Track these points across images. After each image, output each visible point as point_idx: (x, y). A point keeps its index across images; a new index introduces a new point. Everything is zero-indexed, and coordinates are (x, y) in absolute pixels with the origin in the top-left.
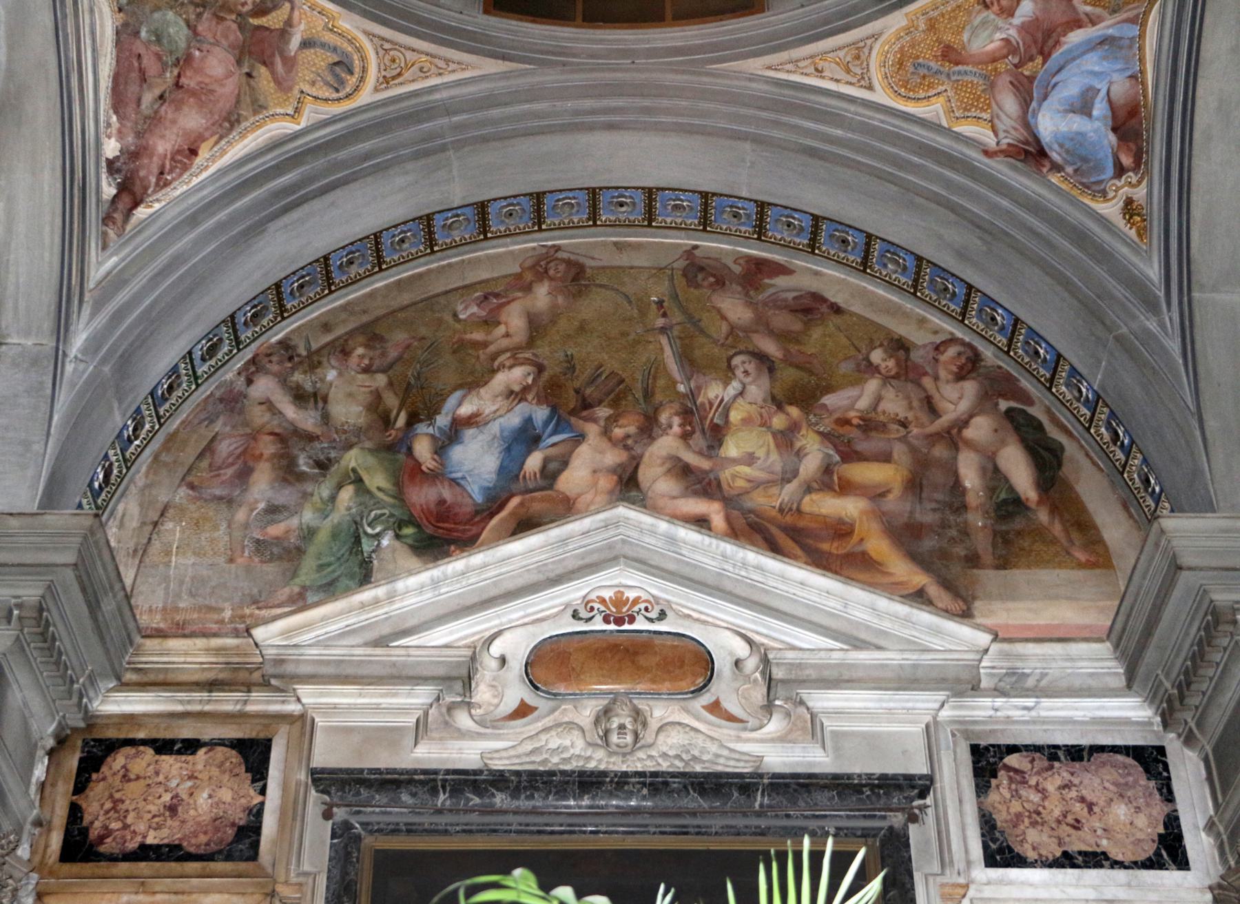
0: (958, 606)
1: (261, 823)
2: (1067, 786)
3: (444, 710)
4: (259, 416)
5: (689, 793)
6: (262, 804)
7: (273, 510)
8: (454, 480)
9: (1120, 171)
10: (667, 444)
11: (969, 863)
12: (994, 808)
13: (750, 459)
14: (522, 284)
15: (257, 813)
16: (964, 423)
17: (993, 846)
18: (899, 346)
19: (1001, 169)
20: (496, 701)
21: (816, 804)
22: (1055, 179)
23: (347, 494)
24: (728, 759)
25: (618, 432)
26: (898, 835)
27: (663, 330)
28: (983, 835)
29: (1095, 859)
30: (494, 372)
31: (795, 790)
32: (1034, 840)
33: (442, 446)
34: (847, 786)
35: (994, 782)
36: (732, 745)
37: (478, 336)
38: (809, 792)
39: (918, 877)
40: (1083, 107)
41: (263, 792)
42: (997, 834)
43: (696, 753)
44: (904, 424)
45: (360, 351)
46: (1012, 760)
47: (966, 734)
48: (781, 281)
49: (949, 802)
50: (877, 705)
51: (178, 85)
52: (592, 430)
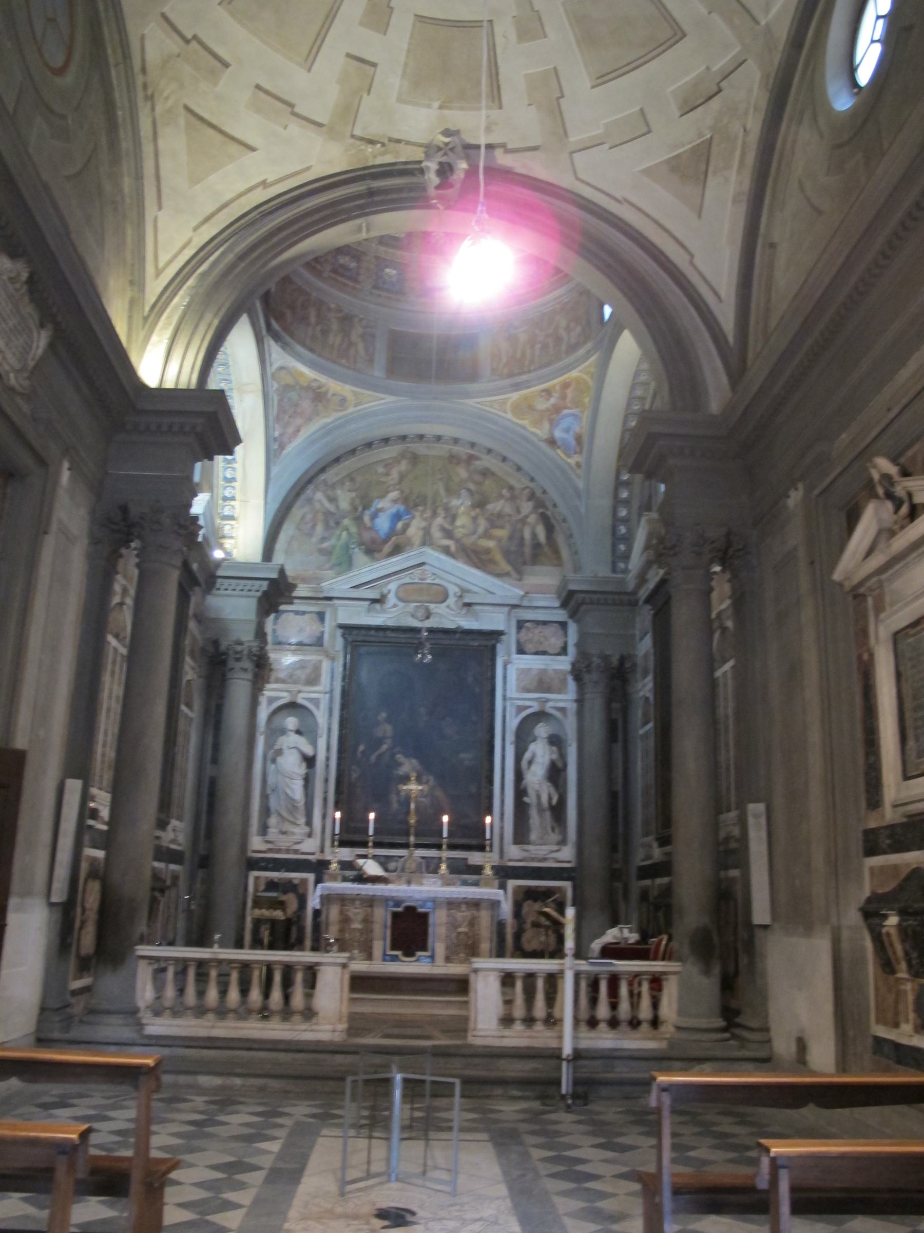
0: (518, 577)
2: (540, 632)
4: (317, 506)
7: (323, 539)
8: (375, 530)
9: (576, 453)
10: (439, 520)
13: (463, 527)
14: (397, 460)
15: (323, 633)
16: (527, 517)
18: (511, 488)
19: (543, 446)
22: (559, 451)
23: (344, 534)
25: (425, 515)
27: (441, 479)
29: (544, 653)
30: (388, 492)
32: (529, 647)
33: (374, 516)
37: (383, 479)
40: (567, 430)
44: (510, 516)
45: (348, 483)
46: (528, 625)
48: (478, 463)
51: (295, 412)
52: (417, 514)
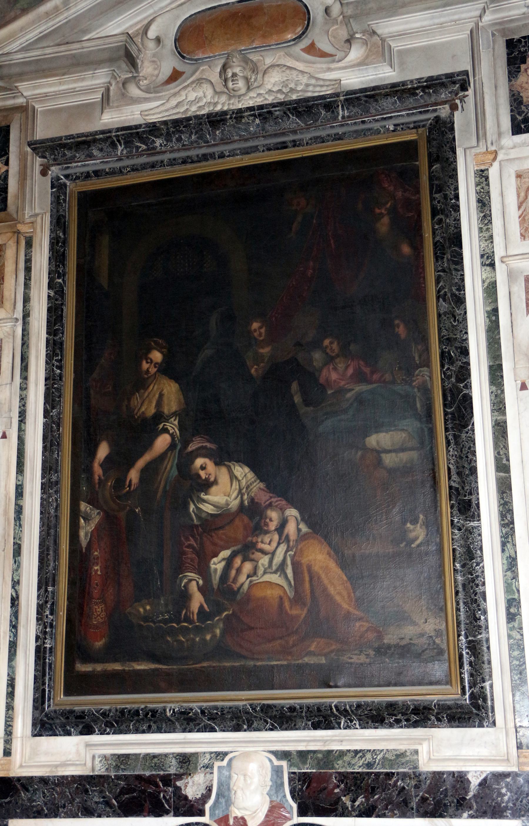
1: (7, 185)
3: (121, 85)
5: (289, 117)
6: (7, 171)
11: (500, 135)
12: (522, 88)
17: (520, 118)
20: (156, 72)
21: (383, 109)
24: (315, 86)
26: (445, 123)
28: (512, 111)
31: (366, 102)
34: (403, 91)
35: (523, 67)
36: (321, 76)
38: (376, 101)
39: (459, 152)
41: (7, 163)
42: (523, 108)
43: (292, 85)
47: (503, 32)
49: (486, 90)
50: (431, 22)
